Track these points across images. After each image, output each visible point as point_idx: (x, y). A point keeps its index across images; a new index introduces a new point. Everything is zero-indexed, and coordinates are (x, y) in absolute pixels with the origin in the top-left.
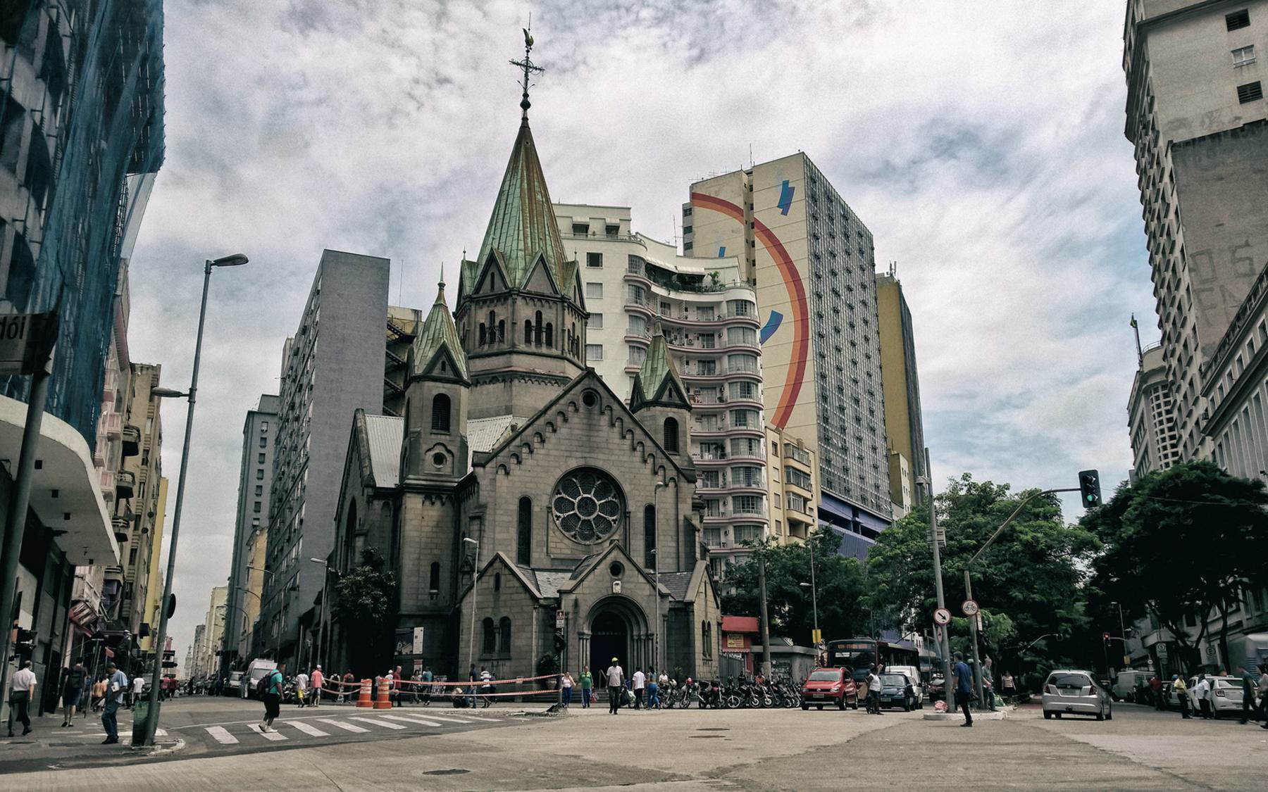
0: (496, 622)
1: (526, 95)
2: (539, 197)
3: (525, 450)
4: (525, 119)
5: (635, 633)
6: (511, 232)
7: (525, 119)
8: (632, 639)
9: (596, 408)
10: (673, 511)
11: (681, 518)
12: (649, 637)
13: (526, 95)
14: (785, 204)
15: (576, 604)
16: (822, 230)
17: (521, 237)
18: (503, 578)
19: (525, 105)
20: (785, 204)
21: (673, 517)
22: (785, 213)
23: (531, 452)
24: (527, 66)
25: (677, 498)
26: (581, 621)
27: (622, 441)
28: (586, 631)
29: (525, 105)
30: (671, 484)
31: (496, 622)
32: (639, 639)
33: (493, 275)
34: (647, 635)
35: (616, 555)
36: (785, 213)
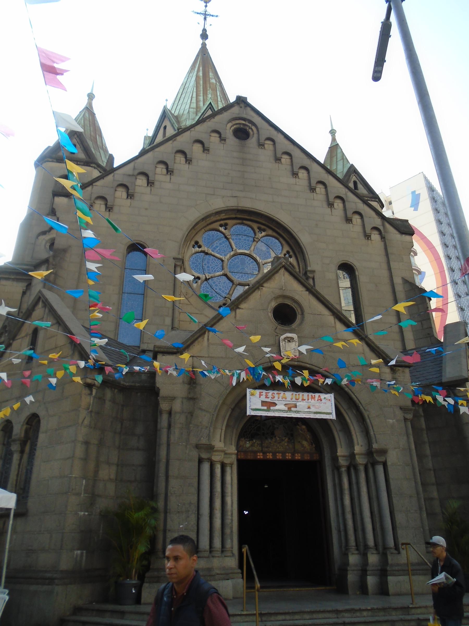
0: (18, 430)
1: (204, 30)
2: (213, 81)
3: (141, 181)
4: (204, 45)
5: (341, 451)
6: (185, 101)
7: (204, 45)
8: (336, 467)
9: (252, 141)
10: (385, 273)
11: (398, 281)
12: (374, 457)
13: (204, 30)
14: (415, 204)
15: (192, 380)
16: (444, 220)
17: (194, 100)
18: (41, 335)
19: (204, 36)
20: (415, 204)
21: (386, 280)
22: (416, 209)
23: (150, 183)
24: (205, 15)
25: (387, 255)
26: (204, 419)
27: (292, 180)
28: (218, 444)
29: (204, 36)
30: (375, 236)
31: (18, 430)
32: (352, 466)
33: (165, 128)
34: (370, 453)
35: (285, 283)
36: (416, 209)
